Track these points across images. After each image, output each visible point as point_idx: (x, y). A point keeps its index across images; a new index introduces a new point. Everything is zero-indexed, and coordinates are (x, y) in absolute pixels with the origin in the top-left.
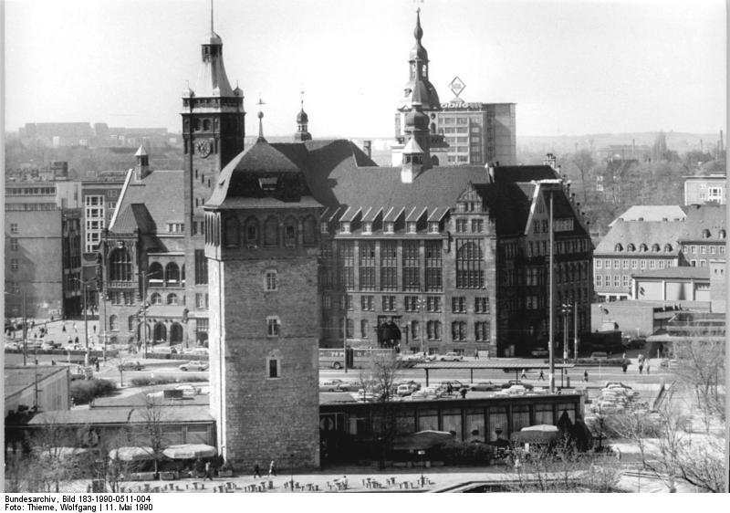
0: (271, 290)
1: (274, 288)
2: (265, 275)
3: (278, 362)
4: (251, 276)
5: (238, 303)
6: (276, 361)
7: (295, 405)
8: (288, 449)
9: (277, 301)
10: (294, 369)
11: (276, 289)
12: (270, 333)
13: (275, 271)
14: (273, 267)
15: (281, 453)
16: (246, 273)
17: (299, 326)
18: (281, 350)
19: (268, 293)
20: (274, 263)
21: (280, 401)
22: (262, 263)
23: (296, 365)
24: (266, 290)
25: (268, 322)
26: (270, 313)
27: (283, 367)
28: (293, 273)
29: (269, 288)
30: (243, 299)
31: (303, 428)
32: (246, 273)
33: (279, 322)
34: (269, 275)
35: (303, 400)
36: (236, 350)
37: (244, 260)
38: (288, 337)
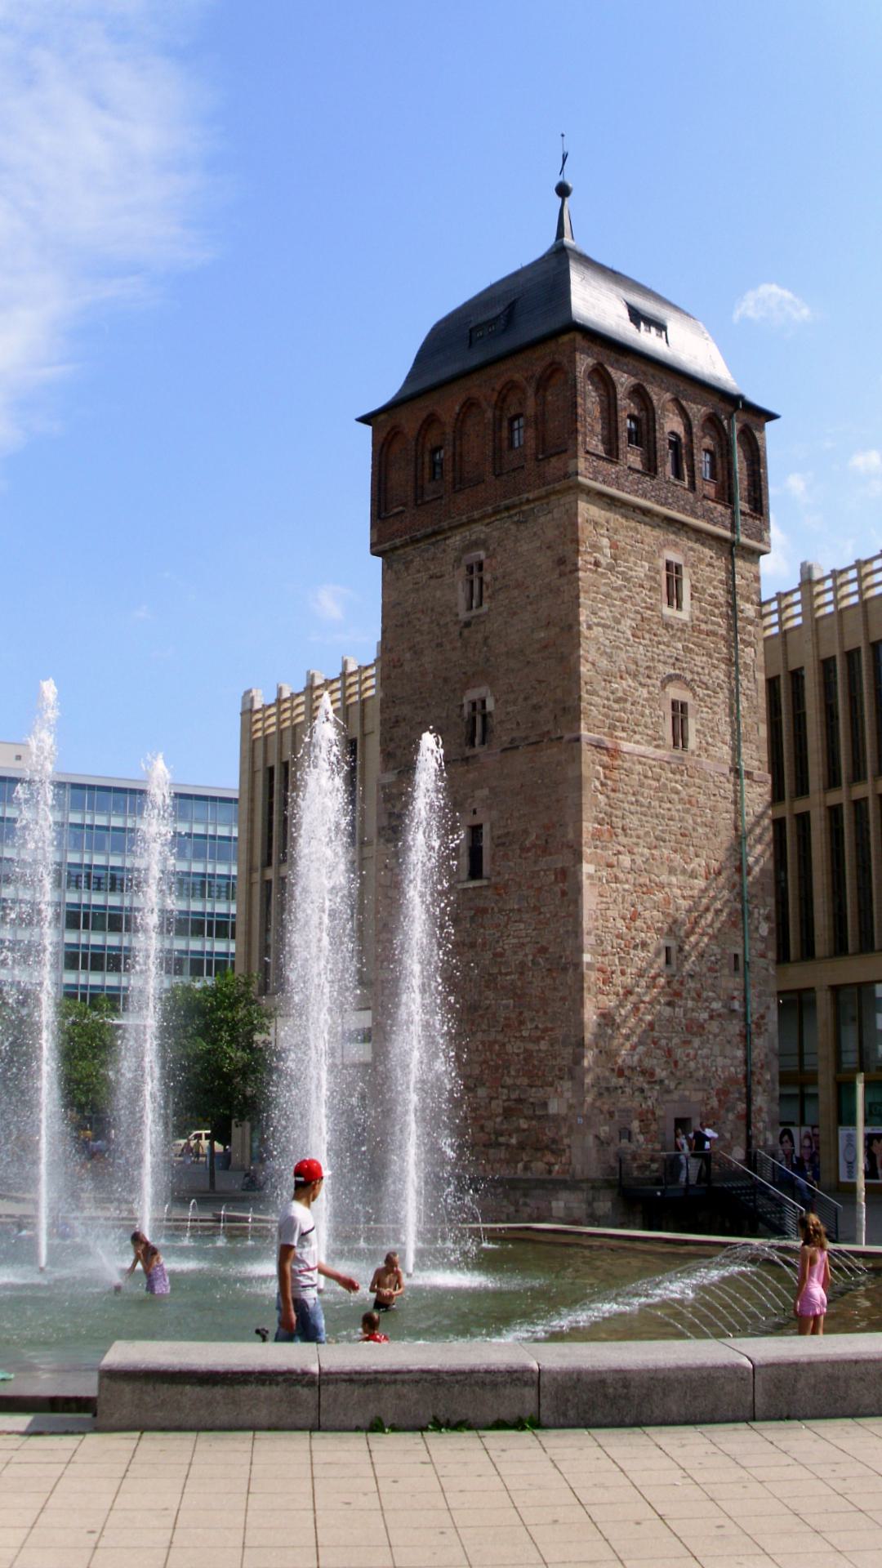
0: (475, 612)
1: (480, 604)
2: (463, 570)
3: (486, 829)
4: (433, 582)
5: (407, 668)
6: (480, 826)
7: (522, 969)
8: (508, 1113)
9: (486, 638)
10: (524, 849)
11: (485, 607)
12: (472, 744)
13: (482, 554)
15: (489, 1125)
16: (424, 576)
17: (536, 708)
18: (492, 789)
19: (467, 624)
20: (479, 531)
21: (489, 955)
22: (456, 540)
23: (526, 832)
24: (464, 615)
25: (467, 709)
26: (466, 686)
27: (499, 843)
28: (524, 547)
29: (470, 608)
30: (417, 652)
31: (544, 1045)
32: (424, 576)
33: (490, 705)
34: (470, 569)
35: (543, 950)
37: (415, 541)
38: (512, 747)
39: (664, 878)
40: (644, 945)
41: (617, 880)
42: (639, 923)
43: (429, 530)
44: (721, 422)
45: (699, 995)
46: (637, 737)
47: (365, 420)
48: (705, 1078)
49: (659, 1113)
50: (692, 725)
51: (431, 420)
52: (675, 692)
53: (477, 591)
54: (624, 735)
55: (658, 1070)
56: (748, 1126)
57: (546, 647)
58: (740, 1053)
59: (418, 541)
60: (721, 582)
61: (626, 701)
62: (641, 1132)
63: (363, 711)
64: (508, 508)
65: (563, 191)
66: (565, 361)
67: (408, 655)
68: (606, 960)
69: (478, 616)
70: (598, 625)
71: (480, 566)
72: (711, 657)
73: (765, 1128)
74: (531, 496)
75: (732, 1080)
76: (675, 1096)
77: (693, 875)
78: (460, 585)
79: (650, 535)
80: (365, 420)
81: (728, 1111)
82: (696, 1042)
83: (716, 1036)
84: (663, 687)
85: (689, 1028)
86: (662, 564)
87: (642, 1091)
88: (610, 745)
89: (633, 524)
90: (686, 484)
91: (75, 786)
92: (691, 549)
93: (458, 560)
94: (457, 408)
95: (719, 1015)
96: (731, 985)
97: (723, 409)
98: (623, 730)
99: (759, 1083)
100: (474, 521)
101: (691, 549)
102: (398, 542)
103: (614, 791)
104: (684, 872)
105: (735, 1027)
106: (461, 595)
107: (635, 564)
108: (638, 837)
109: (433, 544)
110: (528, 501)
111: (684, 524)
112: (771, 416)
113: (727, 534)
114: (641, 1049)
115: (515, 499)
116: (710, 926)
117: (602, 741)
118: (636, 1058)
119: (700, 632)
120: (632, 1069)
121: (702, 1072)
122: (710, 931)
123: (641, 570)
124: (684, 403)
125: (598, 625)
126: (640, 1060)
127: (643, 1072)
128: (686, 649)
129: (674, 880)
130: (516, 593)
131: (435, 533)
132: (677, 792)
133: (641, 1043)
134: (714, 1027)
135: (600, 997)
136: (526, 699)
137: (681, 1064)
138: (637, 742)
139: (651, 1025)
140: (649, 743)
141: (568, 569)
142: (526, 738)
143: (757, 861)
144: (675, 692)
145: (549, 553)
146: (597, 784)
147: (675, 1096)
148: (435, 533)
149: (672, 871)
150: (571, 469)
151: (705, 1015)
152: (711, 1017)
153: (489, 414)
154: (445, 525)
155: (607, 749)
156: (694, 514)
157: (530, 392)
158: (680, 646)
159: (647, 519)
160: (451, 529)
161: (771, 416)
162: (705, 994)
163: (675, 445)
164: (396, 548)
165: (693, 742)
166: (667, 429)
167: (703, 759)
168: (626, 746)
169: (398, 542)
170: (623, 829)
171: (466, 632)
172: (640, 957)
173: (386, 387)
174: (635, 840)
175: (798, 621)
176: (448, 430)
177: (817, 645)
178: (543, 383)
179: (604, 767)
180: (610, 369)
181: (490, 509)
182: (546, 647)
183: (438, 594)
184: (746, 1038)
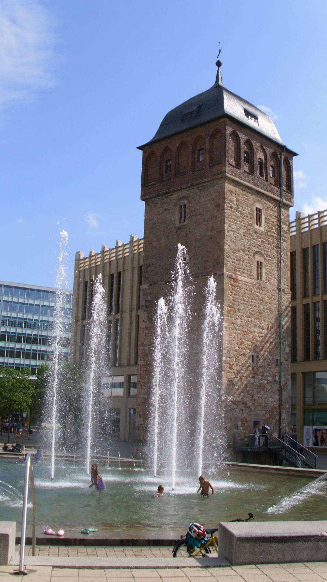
0: (182, 224)
1: (184, 221)
2: (178, 207)
4: (166, 212)
5: (154, 244)
9: (186, 234)
11: (187, 222)
13: (186, 202)
14: (183, 198)
17: (206, 262)
19: (179, 228)
20: (185, 192)
22: (175, 196)
24: (178, 225)
29: (180, 222)
34: (181, 207)
36: (149, 298)
37: (159, 195)
39: (252, 329)
40: (245, 354)
41: (235, 329)
42: (243, 346)
43: (165, 192)
44: (277, 156)
45: (263, 374)
46: (244, 274)
47: (140, 148)
48: (265, 406)
49: (248, 419)
50: (264, 271)
51: (167, 149)
52: (258, 258)
53: (183, 215)
54: (239, 273)
55: (248, 403)
56: (280, 425)
57: (211, 238)
58: (277, 397)
59: (160, 195)
60: (275, 216)
61: (240, 260)
62: (241, 426)
63: (124, 261)
64: (197, 184)
65: (219, 64)
66: (222, 129)
67: (155, 240)
68: (231, 360)
69: (183, 226)
70: (231, 231)
71: (185, 206)
72: (271, 245)
73: (286, 426)
74: (207, 180)
75: (274, 407)
76: (254, 413)
77: (263, 328)
78: (177, 214)
79: (251, 197)
80: (140, 148)
81: (272, 419)
82: (262, 392)
83: (269, 390)
84: (254, 256)
85: (259, 387)
86: (255, 208)
87: (242, 410)
88: (234, 277)
89: (245, 193)
90: (264, 178)
91: (6, 286)
92: (265, 203)
93: (176, 204)
94: (177, 145)
95: (271, 382)
96: (275, 371)
97: (278, 150)
98: (239, 271)
99: (284, 408)
100: (183, 189)
101: (265, 203)
102: (152, 195)
103: (235, 295)
104: (259, 327)
105: (276, 387)
106: (177, 217)
107: (245, 208)
108: (244, 313)
109: (166, 197)
110: (205, 182)
111: (263, 194)
112: (295, 154)
113: (278, 198)
114: (242, 394)
115: (200, 181)
116: (268, 348)
117: (231, 275)
118: (240, 398)
119: (268, 235)
120: (239, 402)
121: (264, 404)
122: (268, 350)
123: (247, 211)
124: (264, 147)
125: (231, 231)
126: (242, 399)
127: (243, 403)
128: (262, 241)
129: (256, 330)
130: (199, 217)
131: (167, 193)
132: (258, 296)
133: (242, 392)
134: (268, 387)
135: (228, 374)
136: (202, 258)
137: (256, 401)
138: (244, 276)
139: (246, 385)
140: (248, 277)
141: (221, 208)
142: (202, 273)
143: (285, 324)
144: (258, 258)
145: (213, 202)
146: (229, 292)
147: (254, 413)
148: (167, 193)
149: (255, 326)
150: (223, 170)
151: (266, 382)
152: (268, 383)
153: (191, 148)
154: (171, 190)
155: (233, 279)
156: (267, 190)
157: (207, 140)
158: (260, 240)
159: (250, 191)
160: (173, 191)
161: (295, 154)
162: (266, 374)
163: (261, 163)
164: (151, 198)
165: (264, 277)
166: (258, 157)
167: (267, 284)
168: (240, 278)
169: (152, 195)
170: (238, 310)
171: (178, 231)
172: (243, 359)
173: (148, 135)
174: (242, 314)
175: (294, 233)
176: (174, 153)
177: (301, 243)
178: (212, 137)
179: (232, 286)
180: (238, 133)
181: (190, 184)
182: (211, 238)
183: (168, 216)
184: (280, 391)
